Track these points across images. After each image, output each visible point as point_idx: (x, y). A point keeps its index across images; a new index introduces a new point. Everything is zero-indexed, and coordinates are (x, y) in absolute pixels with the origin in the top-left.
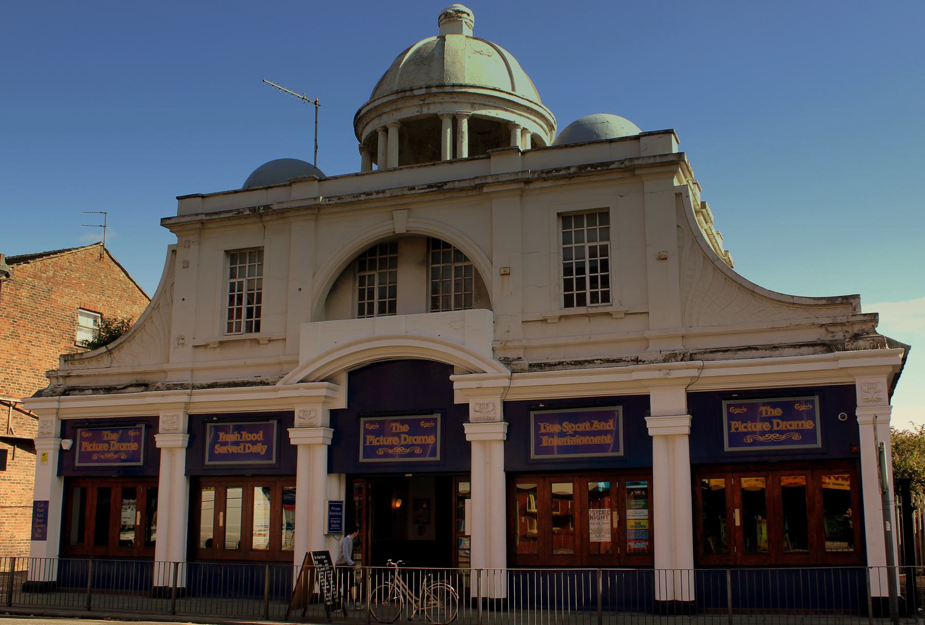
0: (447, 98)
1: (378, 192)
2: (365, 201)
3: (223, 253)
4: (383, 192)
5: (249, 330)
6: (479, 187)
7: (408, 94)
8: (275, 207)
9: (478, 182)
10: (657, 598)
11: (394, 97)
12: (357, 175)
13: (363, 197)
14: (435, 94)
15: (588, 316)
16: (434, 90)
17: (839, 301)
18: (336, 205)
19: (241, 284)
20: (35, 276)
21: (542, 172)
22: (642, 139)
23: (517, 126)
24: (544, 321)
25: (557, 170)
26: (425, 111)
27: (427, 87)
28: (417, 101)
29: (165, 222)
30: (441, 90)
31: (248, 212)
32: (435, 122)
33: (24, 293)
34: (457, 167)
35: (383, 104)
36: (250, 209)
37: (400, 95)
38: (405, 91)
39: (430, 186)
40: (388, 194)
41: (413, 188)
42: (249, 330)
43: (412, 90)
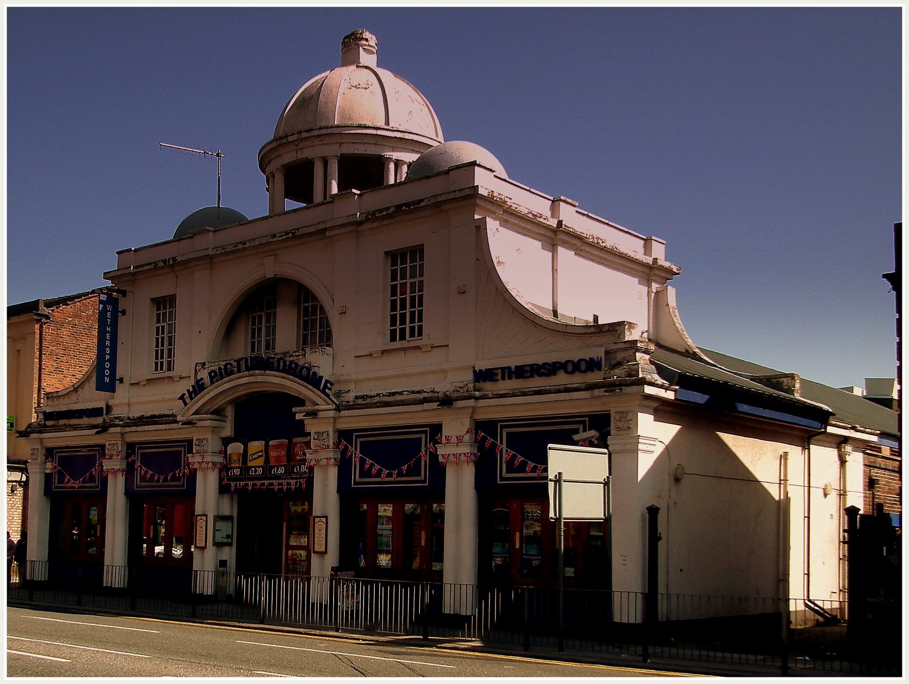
0: (317, 141)
3: (149, 301)
6: (322, 232)
7: (284, 141)
9: (320, 227)
12: (267, 217)
14: (306, 139)
15: (404, 349)
16: (304, 135)
17: (606, 328)
19: (163, 327)
20: (75, 316)
23: (390, 159)
24: (371, 355)
25: (380, 211)
26: (300, 156)
27: (298, 133)
30: (309, 134)
31: (161, 264)
32: (307, 166)
33: (65, 332)
36: (162, 261)
41: (274, 236)
42: (169, 369)
43: (286, 136)
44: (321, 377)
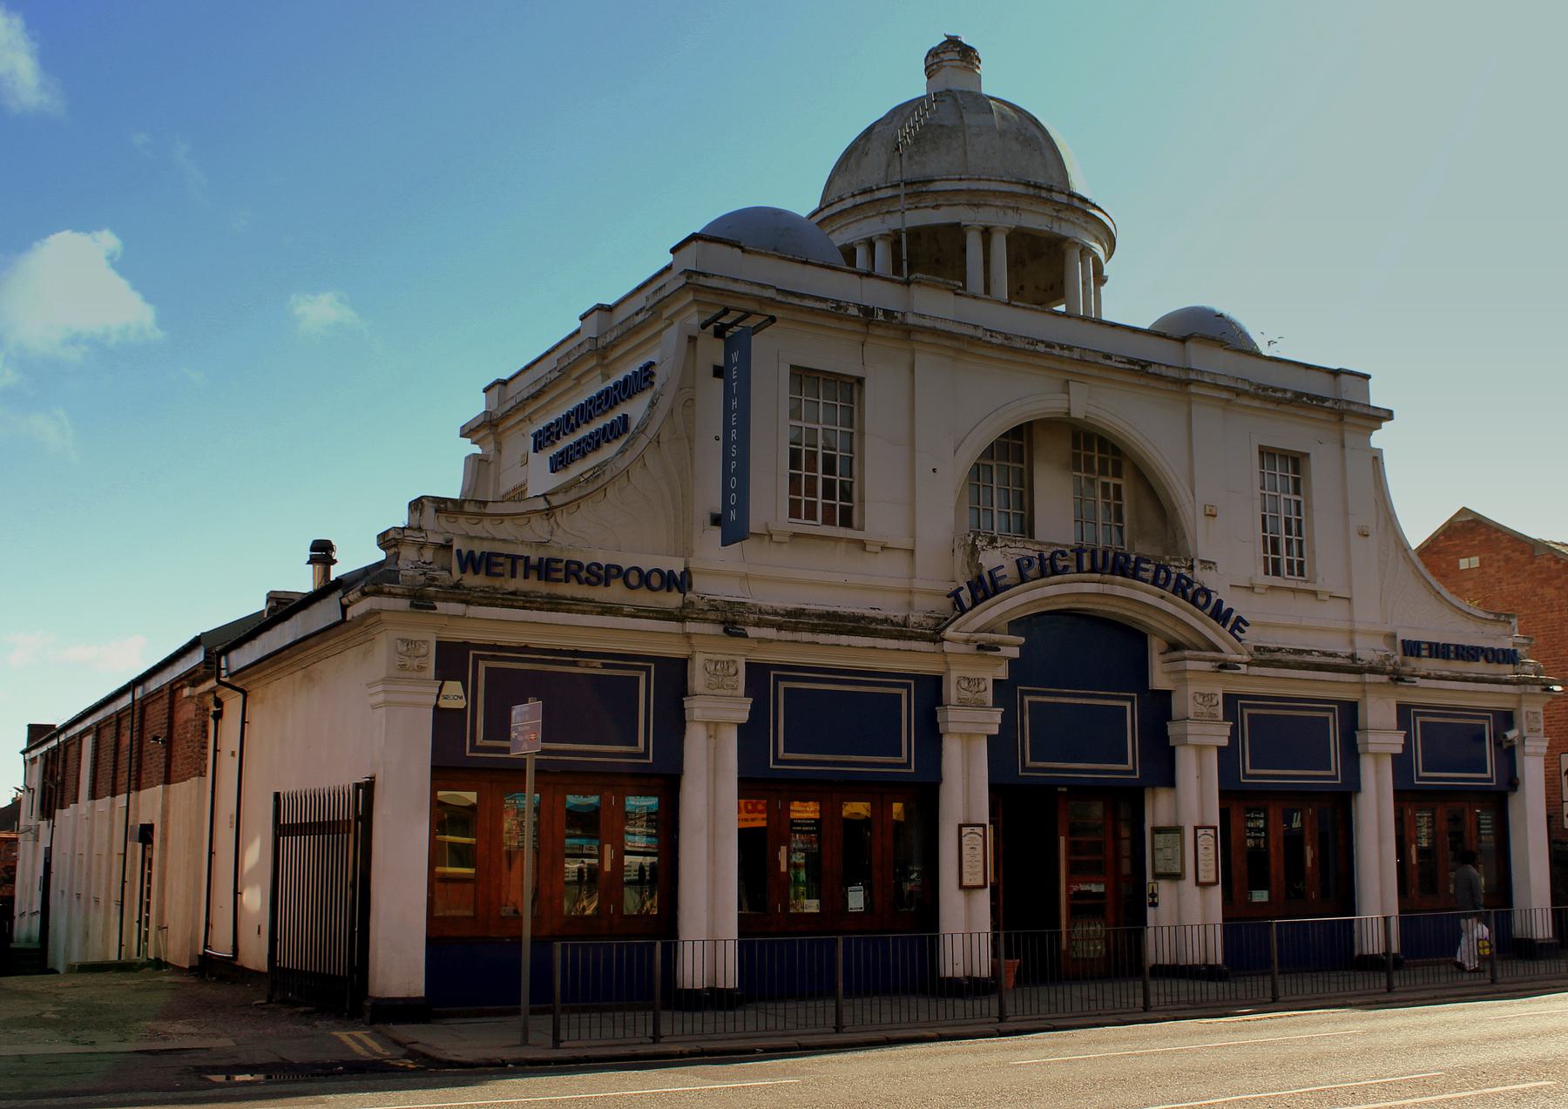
0: (1081, 221)
1: (1062, 347)
2: (1037, 354)
4: (1070, 348)
5: (828, 520)
6: (1188, 382)
7: (1044, 194)
8: (911, 320)
10: (679, 986)
11: (1020, 189)
13: (1041, 348)
18: (1001, 347)
21: (1258, 386)
22: (1344, 377)
25: (1275, 390)
26: (1056, 229)
28: (1048, 210)
29: (1389, 415)
31: (853, 311)
34: (869, 283)
35: (995, 193)
37: (1031, 191)
38: (1040, 188)
39: (1131, 361)
40: (1076, 355)
43: (1050, 190)
44: (1230, 611)
